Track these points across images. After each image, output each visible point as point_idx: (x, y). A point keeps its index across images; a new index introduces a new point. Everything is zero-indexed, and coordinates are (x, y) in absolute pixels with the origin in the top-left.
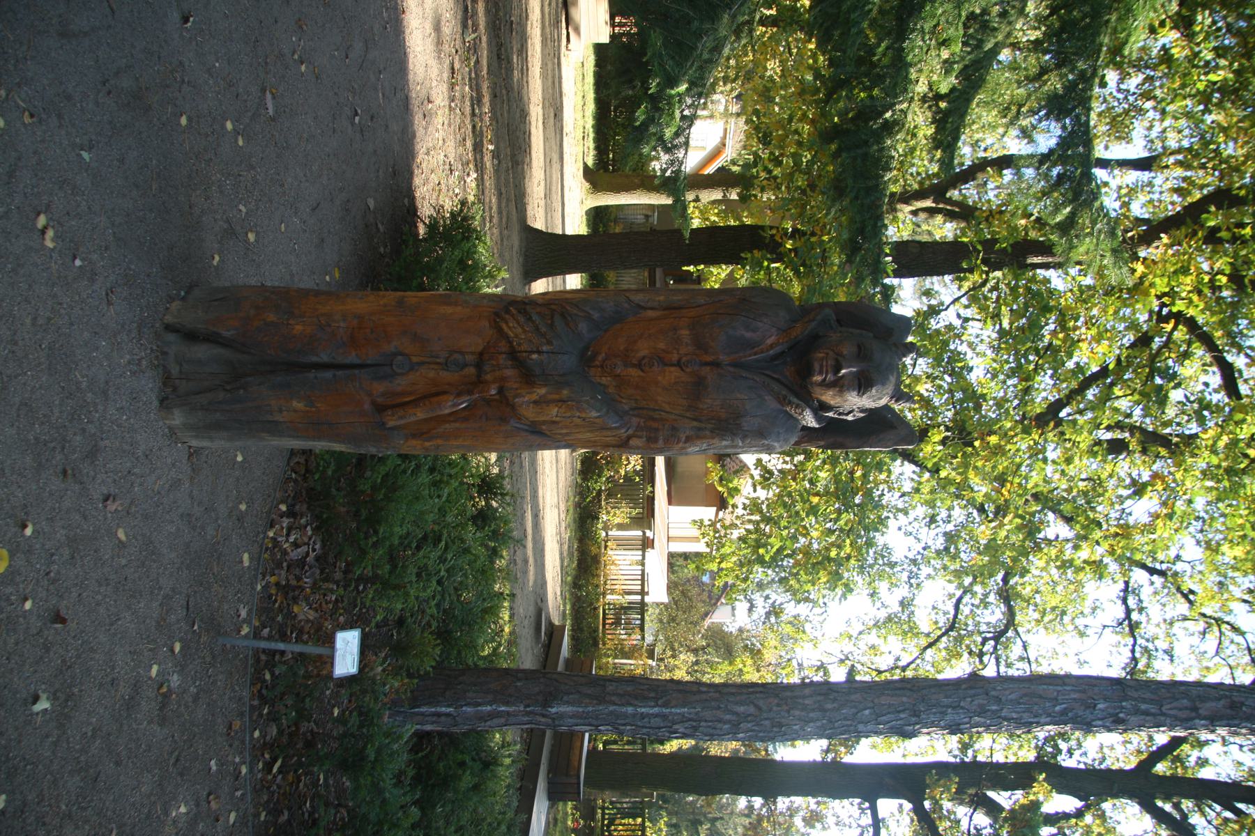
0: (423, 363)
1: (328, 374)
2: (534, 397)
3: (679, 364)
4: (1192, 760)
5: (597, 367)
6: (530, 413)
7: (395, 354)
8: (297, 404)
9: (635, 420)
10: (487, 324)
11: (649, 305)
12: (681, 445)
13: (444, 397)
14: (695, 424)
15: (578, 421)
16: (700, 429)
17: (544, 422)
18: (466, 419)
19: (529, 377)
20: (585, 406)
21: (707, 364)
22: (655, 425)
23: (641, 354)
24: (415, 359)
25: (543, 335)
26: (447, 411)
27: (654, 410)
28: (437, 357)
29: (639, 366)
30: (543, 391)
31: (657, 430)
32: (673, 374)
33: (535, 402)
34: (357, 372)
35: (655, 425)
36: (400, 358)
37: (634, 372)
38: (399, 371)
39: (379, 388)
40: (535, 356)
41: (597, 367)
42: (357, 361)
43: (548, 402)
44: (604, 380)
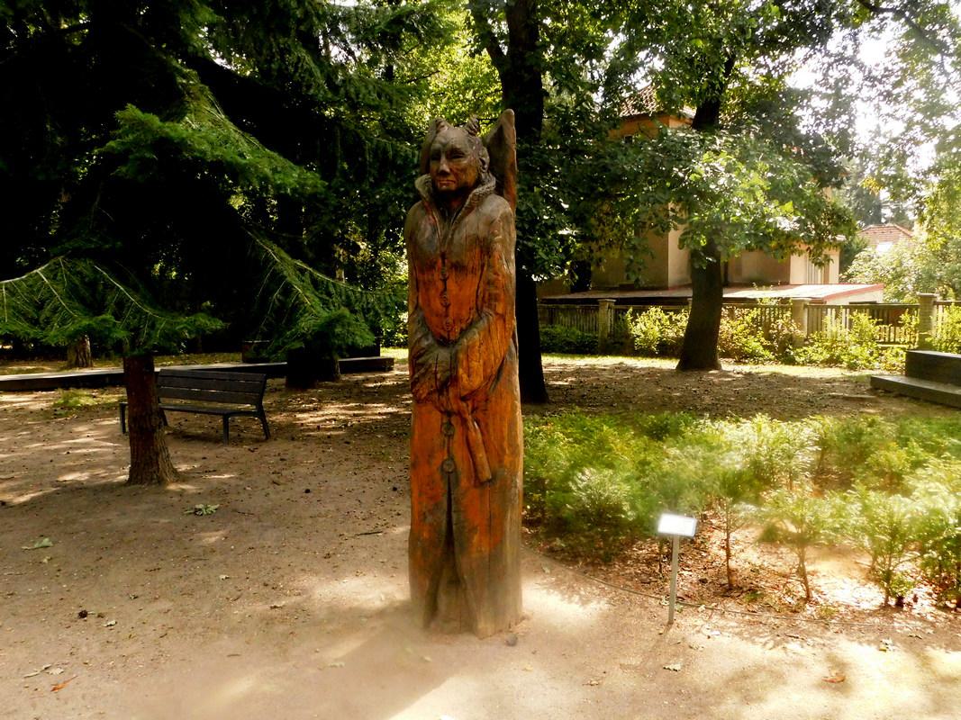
0: (448, 451)
1: (454, 516)
2: (465, 376)
3: (444, 281)
4: (824, 353)
5: (449, 335)
6: (477, 381)
7: (442, 470)
8: (476, 539)
9: (485, 309)
10: (424, 408)
11: (416, 301)
12: (500, 278)
13: (470, 438)
14: (485, 269)
15: (483, 348)
16: (489, 266)
17: (485, 370)
18: (487, 425)
19: (453, 380)
20: (471, 343)
21: (444, 263)
22: (487, 295)
23: (439, 306)
24: (446, 457)
25: (427, 370)
26: (480, 436)
27: (477, 296)
28: (444, 442)
29: (447, 307)
30: (461, 371)
31: (490, 295)
32: (451, 284)
33: (469, 376)
34: (453, 497)
35: (487, 295)
36: (445, 466)
37: (451, 310)
38: (453, 467)
39: (464, 483)
40: (439, 376)
41: (449, 335)
42: (446, 497)
43: (469, 367)
44: (458, 330)
